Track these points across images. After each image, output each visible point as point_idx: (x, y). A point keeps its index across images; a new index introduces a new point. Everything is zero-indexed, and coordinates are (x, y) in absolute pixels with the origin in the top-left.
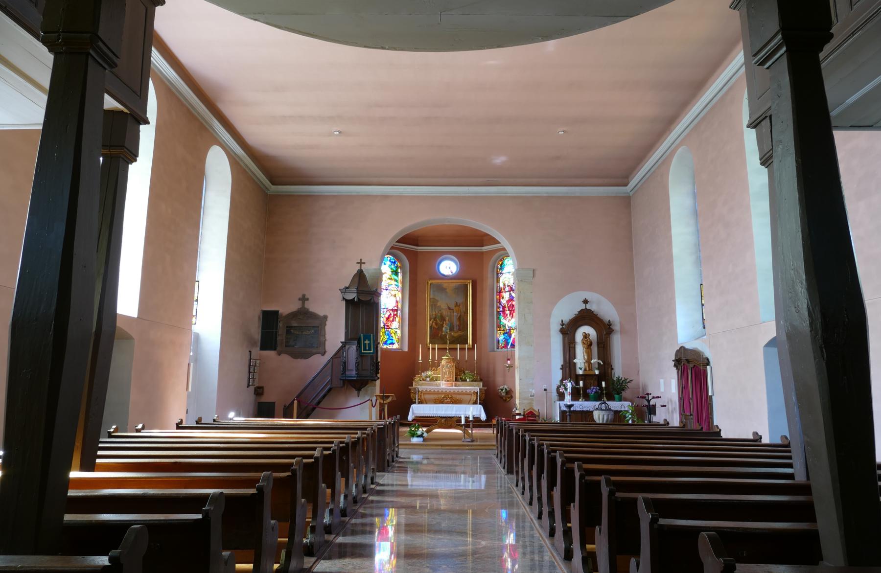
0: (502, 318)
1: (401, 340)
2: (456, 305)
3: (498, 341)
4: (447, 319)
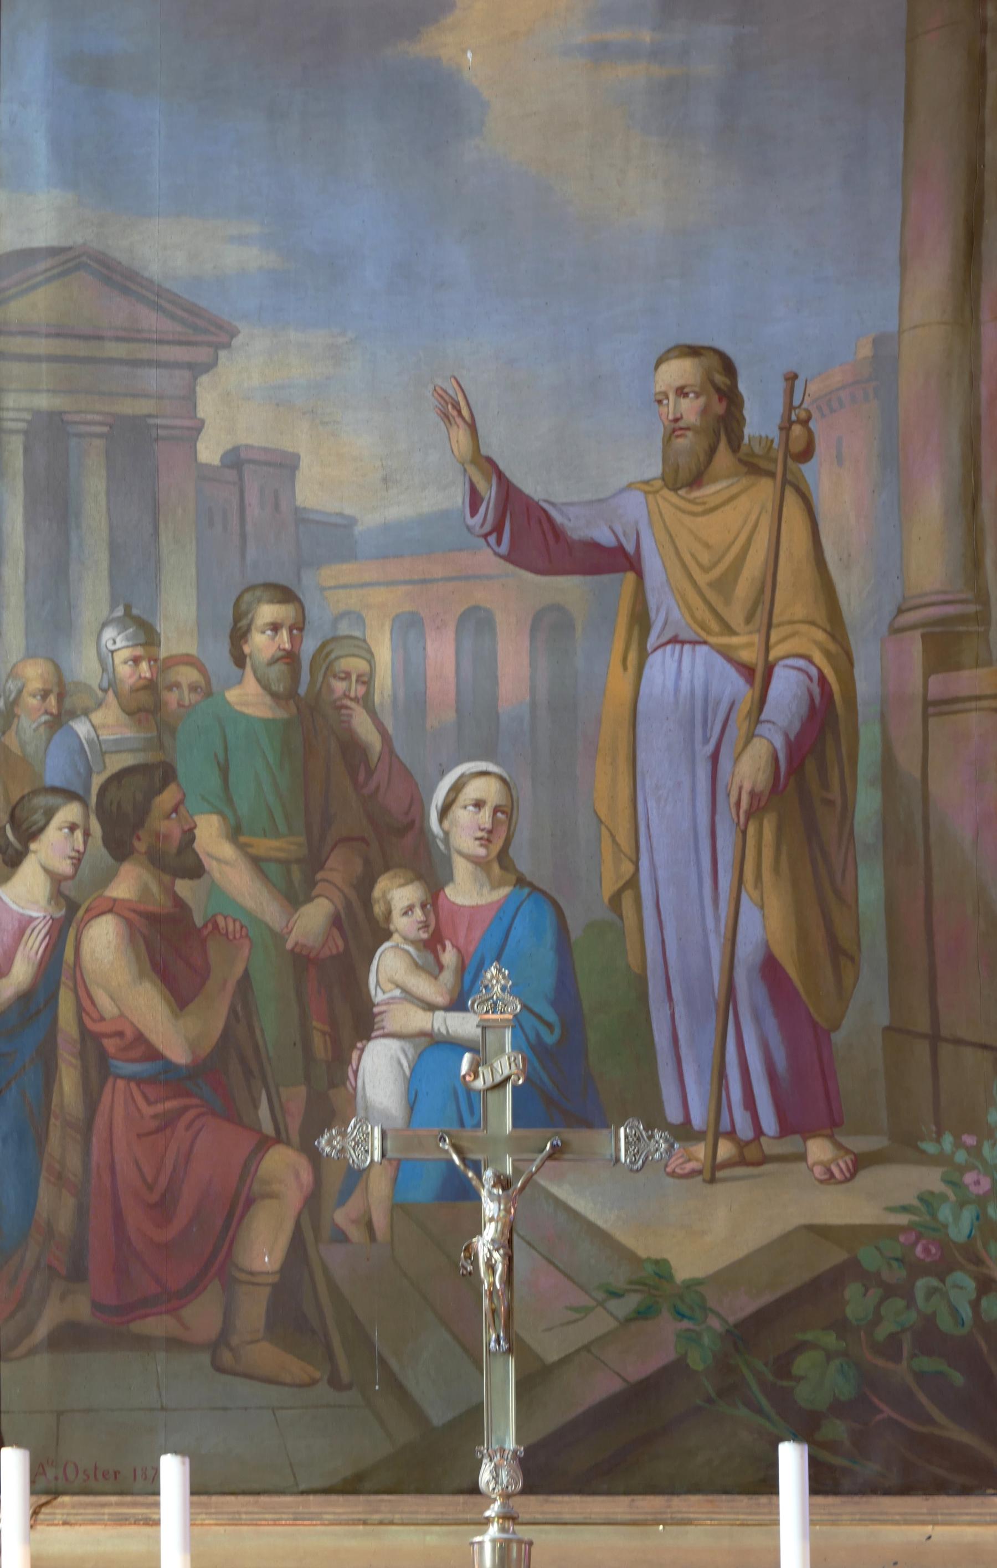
4: (463, 805)
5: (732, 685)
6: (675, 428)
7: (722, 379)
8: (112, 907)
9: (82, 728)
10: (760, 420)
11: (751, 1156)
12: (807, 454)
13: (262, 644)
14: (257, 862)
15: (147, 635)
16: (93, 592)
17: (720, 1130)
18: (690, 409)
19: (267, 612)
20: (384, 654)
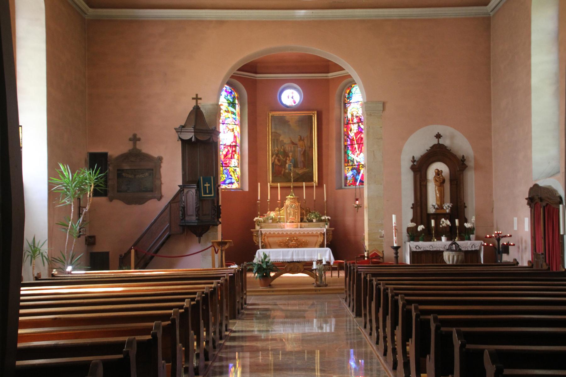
0: (350, 152)
1: (241, 179)
2: (301, 139)
3: (346, 178)
4: (290, 154)
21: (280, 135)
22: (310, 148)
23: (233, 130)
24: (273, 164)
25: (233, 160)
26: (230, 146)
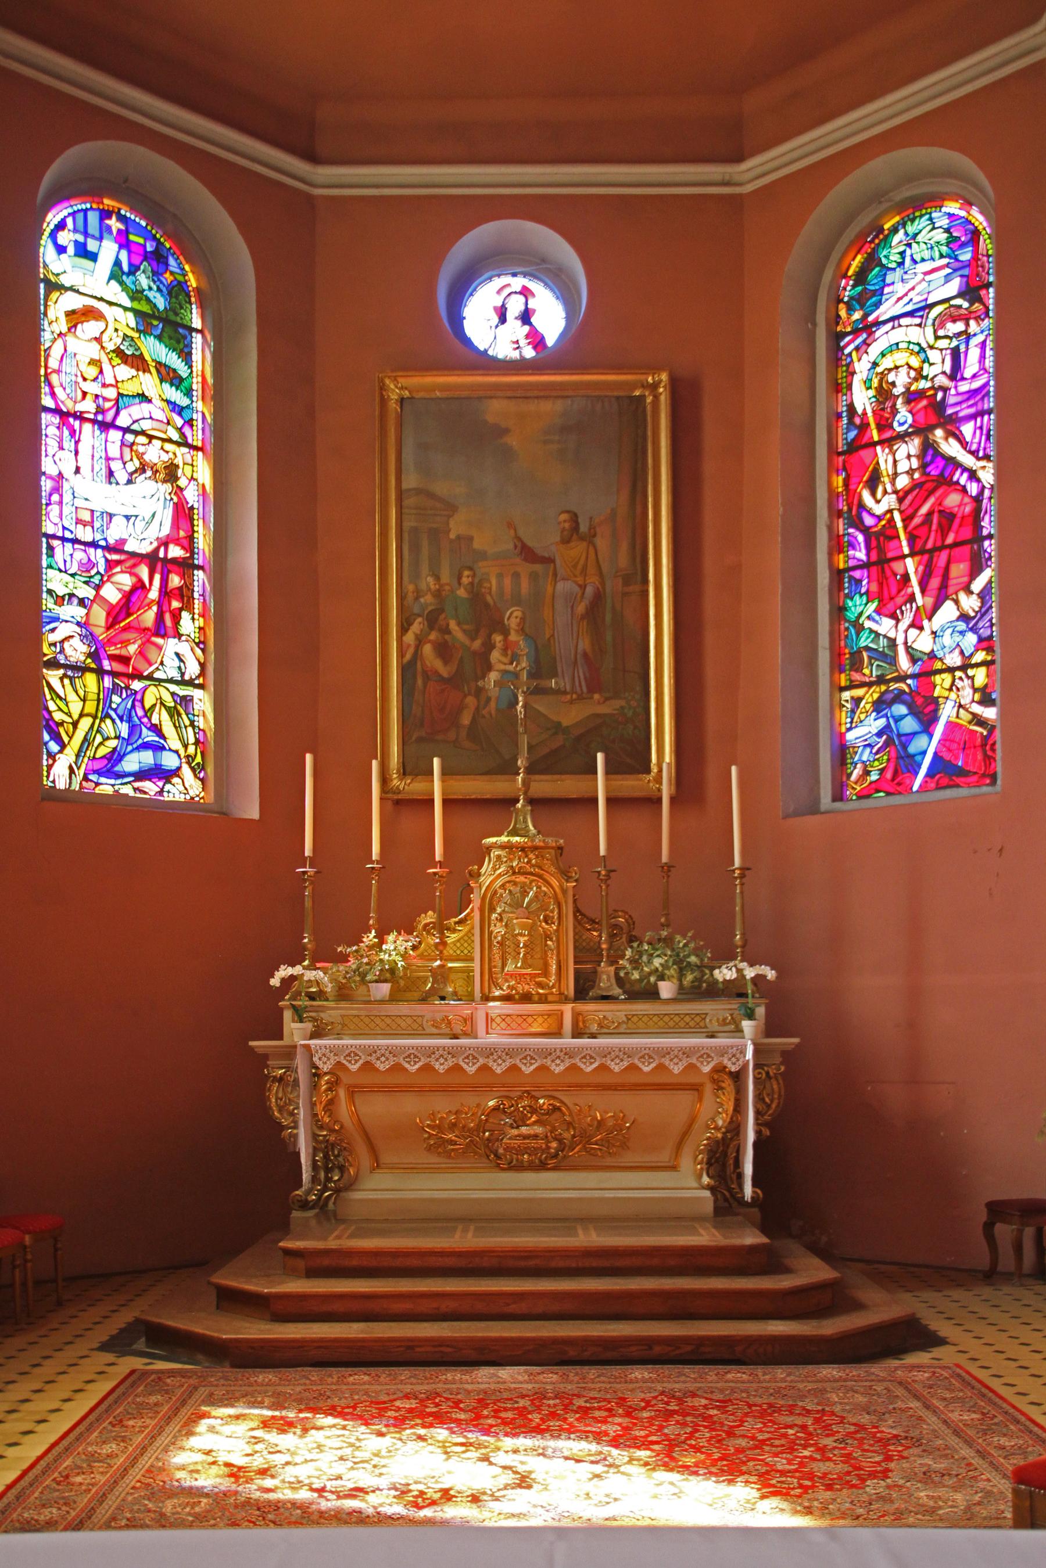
2: (573, 532)
4: (513, 617)
5: (576, 589)
6: (563, 530)
7: (574, 518)
8: (430, 641)
9: (422, 600)
10: (583, 528)
11: (580, 698)
12: (595, 536)
13: (465, 580)
14: (464, 631)
15: (437, 578)
16: (425, 569)
17: (573, 692)
18: (567, 525)
19: (466, 573)
20: (494, 582)
21: (452, 508)
22: (627, 580)
23: (170, 473)
24: (407, 670)
25: (171, 646)
26: (151, 559)
